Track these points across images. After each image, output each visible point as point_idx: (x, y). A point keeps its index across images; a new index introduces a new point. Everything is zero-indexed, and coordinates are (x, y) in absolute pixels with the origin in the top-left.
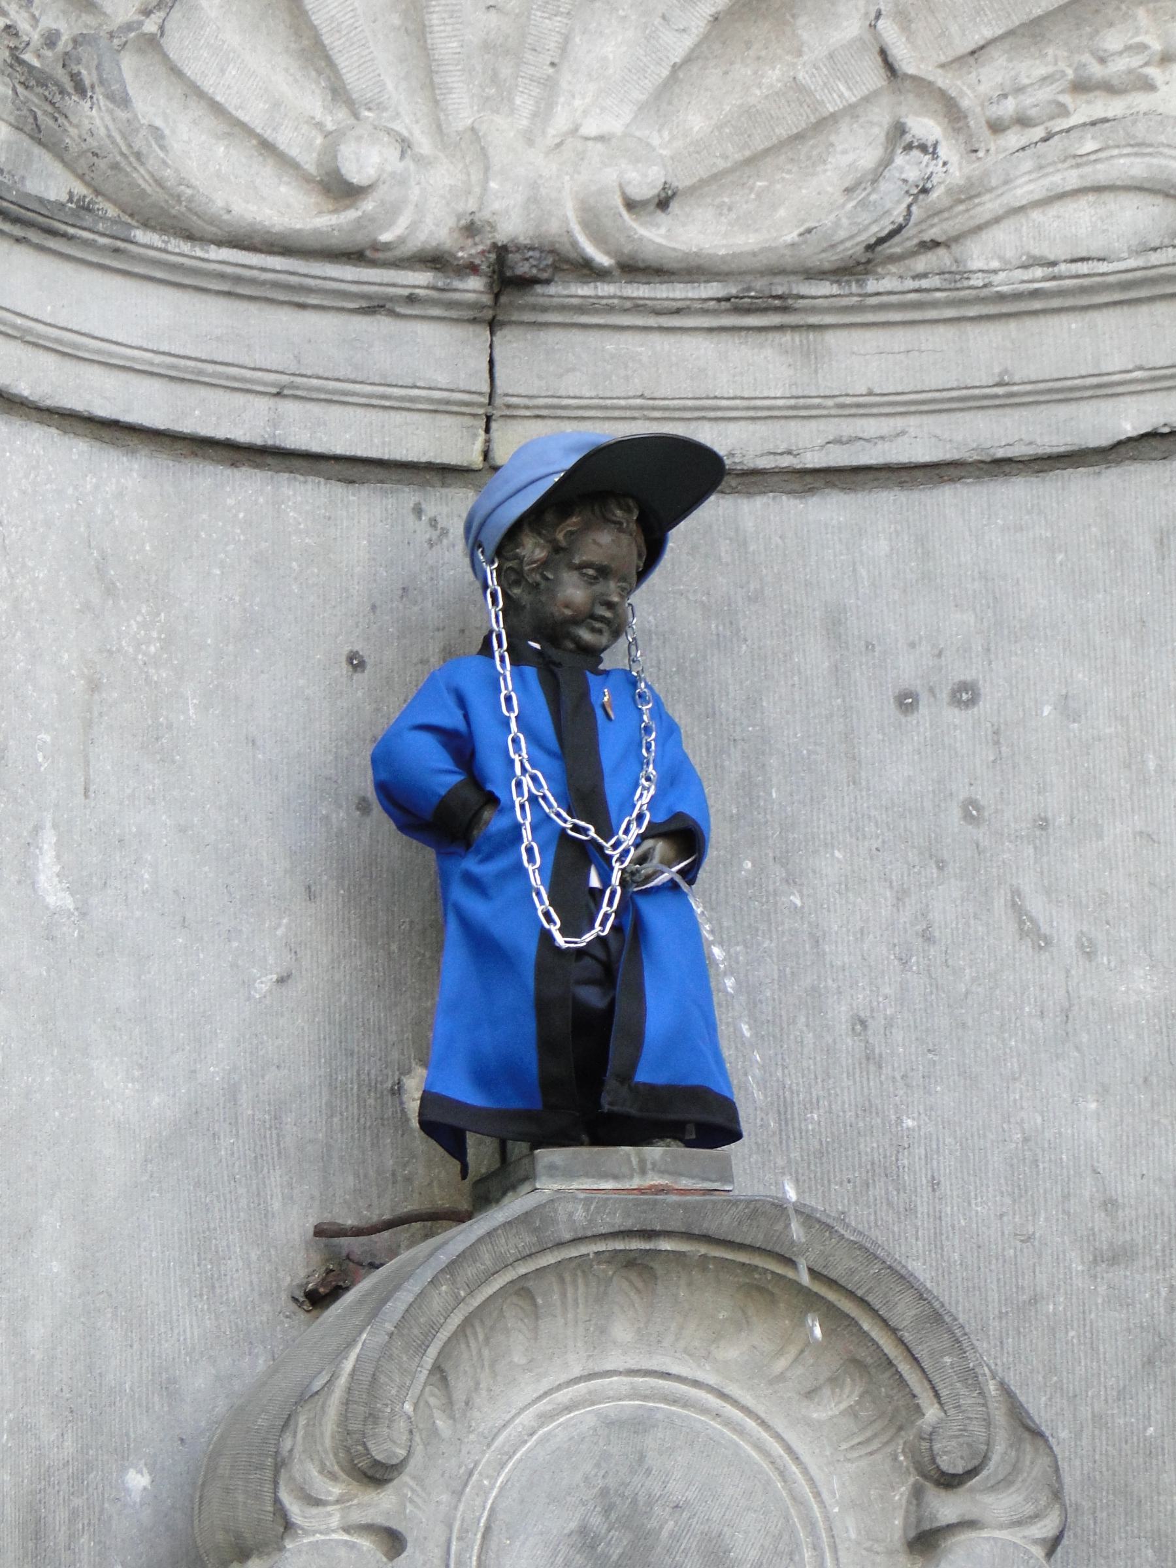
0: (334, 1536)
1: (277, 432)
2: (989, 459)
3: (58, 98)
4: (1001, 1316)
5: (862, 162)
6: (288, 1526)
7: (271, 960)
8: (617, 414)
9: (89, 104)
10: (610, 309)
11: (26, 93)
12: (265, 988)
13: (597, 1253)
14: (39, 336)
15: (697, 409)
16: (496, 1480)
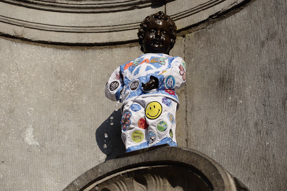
1: (110, 39)
13: (122, 174)
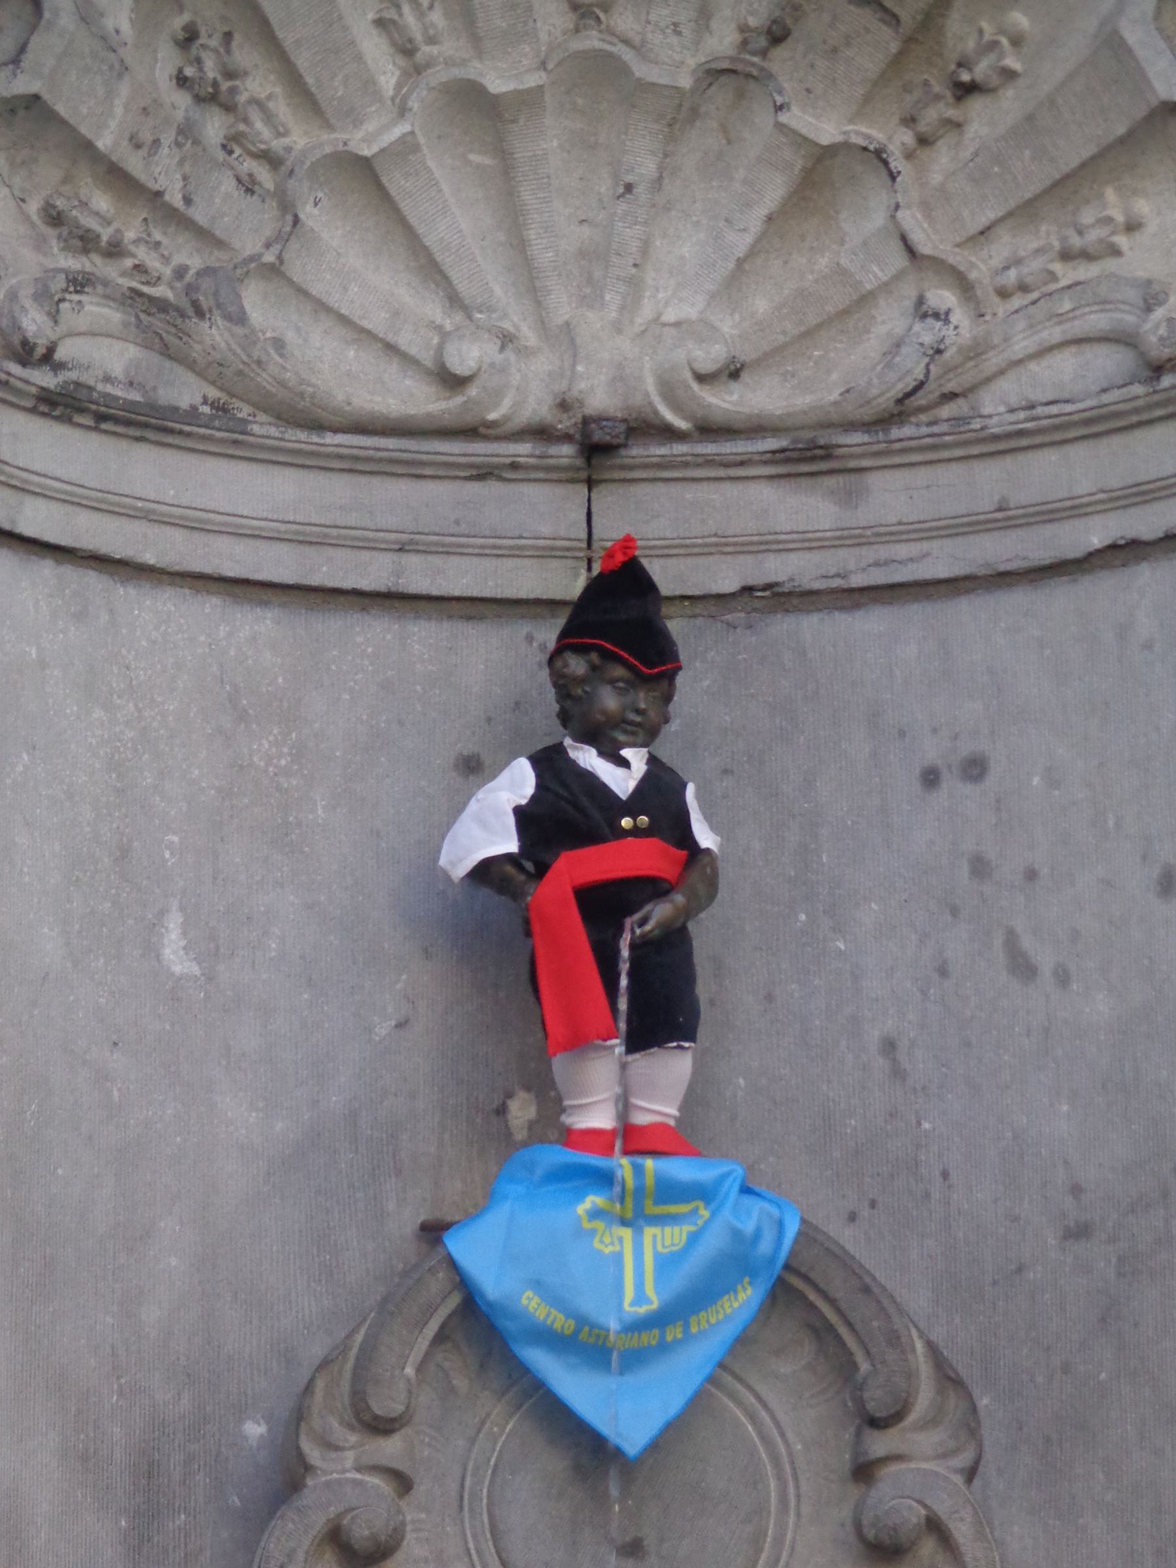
0: (348, 1475)
2: (994, 573)
3: (179, 321)
4: (995, 1283)
5: (897, 330)
6: (308, 1468)
7: (390, 1010)
8: (696, 550)
9: (208, 324)
10: (686, 465)
11: (150, 319)
12: (383, 1032)
14: (164, 515)
15: (761, 543)
16: (505, 1427)
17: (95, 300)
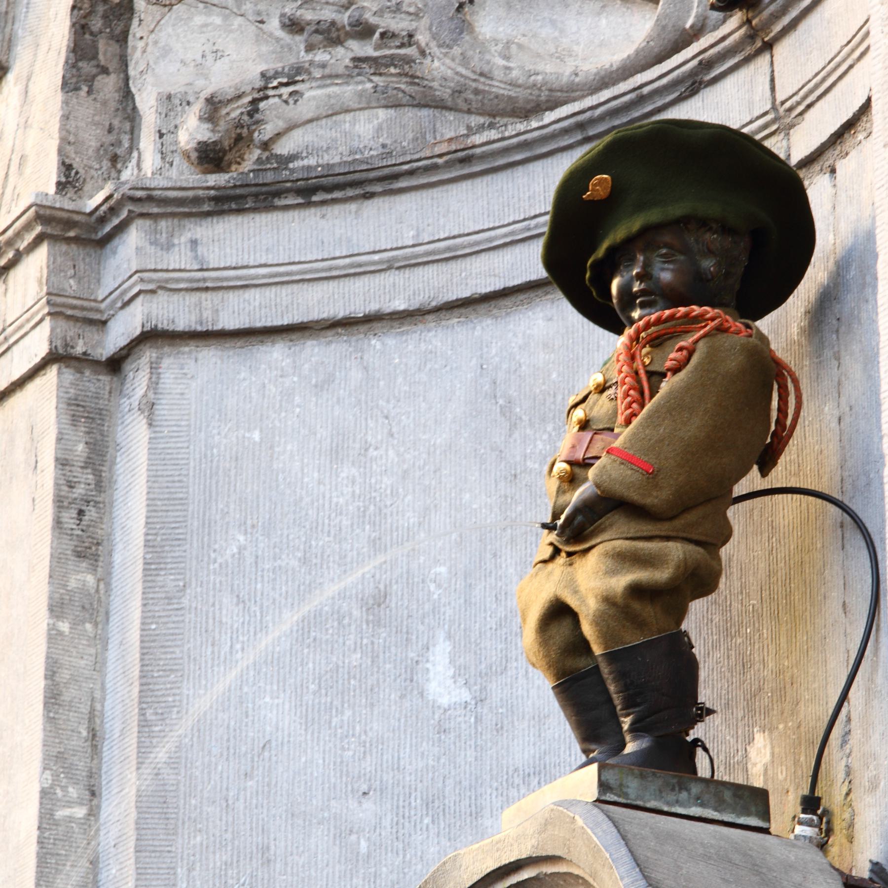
14: (406, 258)
17: (314, 84)
